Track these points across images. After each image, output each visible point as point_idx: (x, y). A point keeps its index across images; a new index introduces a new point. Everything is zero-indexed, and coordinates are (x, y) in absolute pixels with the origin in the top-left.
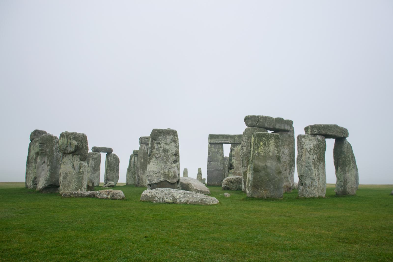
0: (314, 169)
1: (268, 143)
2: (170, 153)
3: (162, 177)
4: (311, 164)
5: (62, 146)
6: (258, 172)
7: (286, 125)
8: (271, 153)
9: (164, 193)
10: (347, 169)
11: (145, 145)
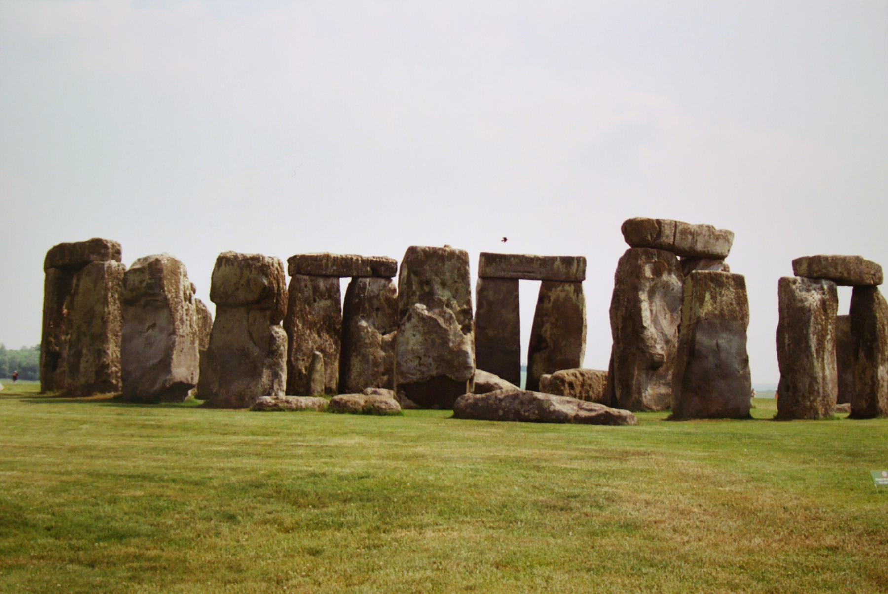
3: (434, 365)
5: (222, 289)
9: (517, 401)
11: (307, 278)
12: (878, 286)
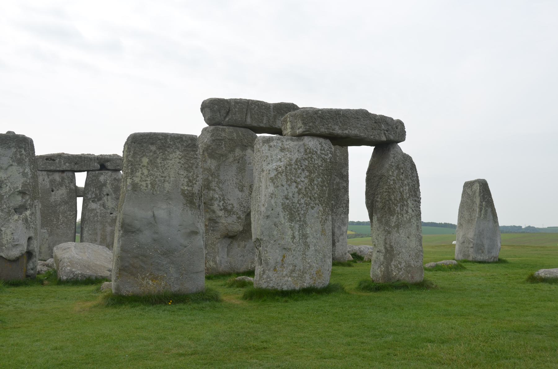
0: (287, 224)
1: (164, 159)
2: (7, 190)
4: (279, 209)
6: (133, 232)
8: (169, 183)
10: (394, 220)
11: (45, 173)
12: (399, 144)
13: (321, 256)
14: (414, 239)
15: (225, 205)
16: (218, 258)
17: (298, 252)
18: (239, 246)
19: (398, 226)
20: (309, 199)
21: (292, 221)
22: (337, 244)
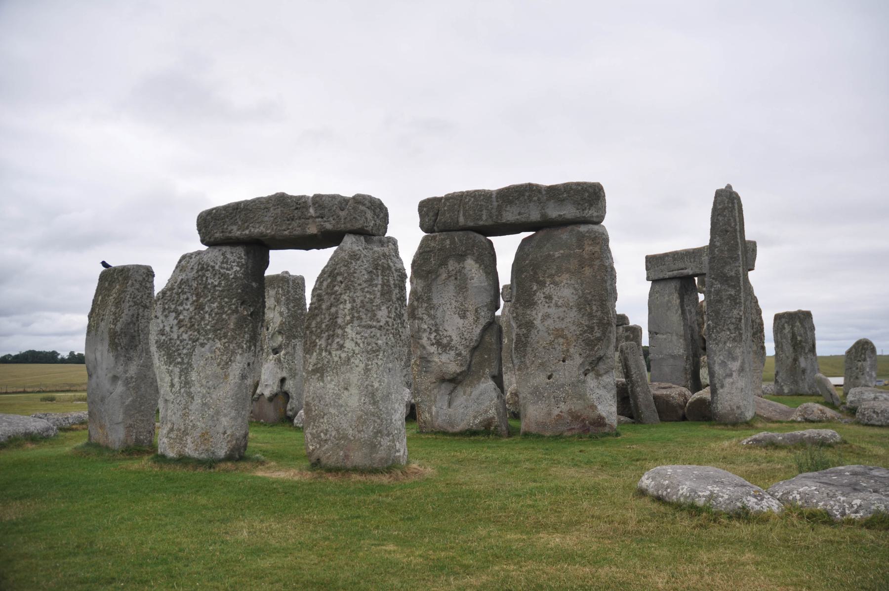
0: (164, 368)
7: (551, 204)
13: (211, 412)
14: (357, 392)
15: (438, 337)
16: (434, 409)
17: (177, 406)
18: (464, 393)
19: (320, 371)
20: (196, 333)
21: (171, 363)
22: (720, 391)
